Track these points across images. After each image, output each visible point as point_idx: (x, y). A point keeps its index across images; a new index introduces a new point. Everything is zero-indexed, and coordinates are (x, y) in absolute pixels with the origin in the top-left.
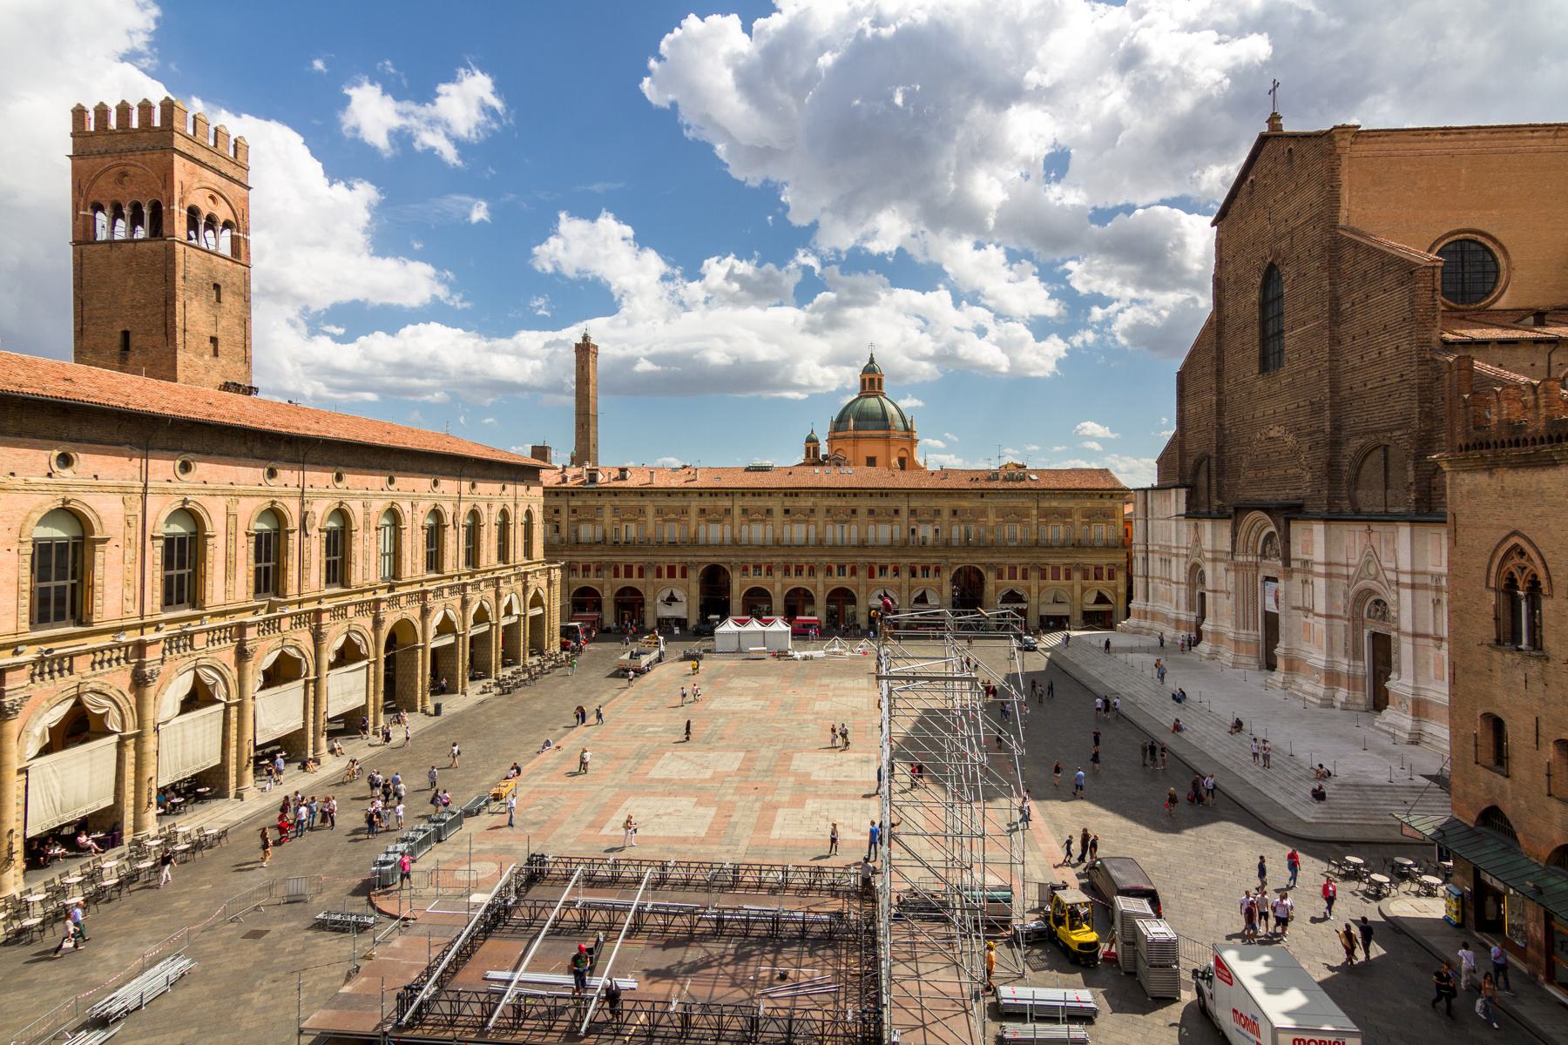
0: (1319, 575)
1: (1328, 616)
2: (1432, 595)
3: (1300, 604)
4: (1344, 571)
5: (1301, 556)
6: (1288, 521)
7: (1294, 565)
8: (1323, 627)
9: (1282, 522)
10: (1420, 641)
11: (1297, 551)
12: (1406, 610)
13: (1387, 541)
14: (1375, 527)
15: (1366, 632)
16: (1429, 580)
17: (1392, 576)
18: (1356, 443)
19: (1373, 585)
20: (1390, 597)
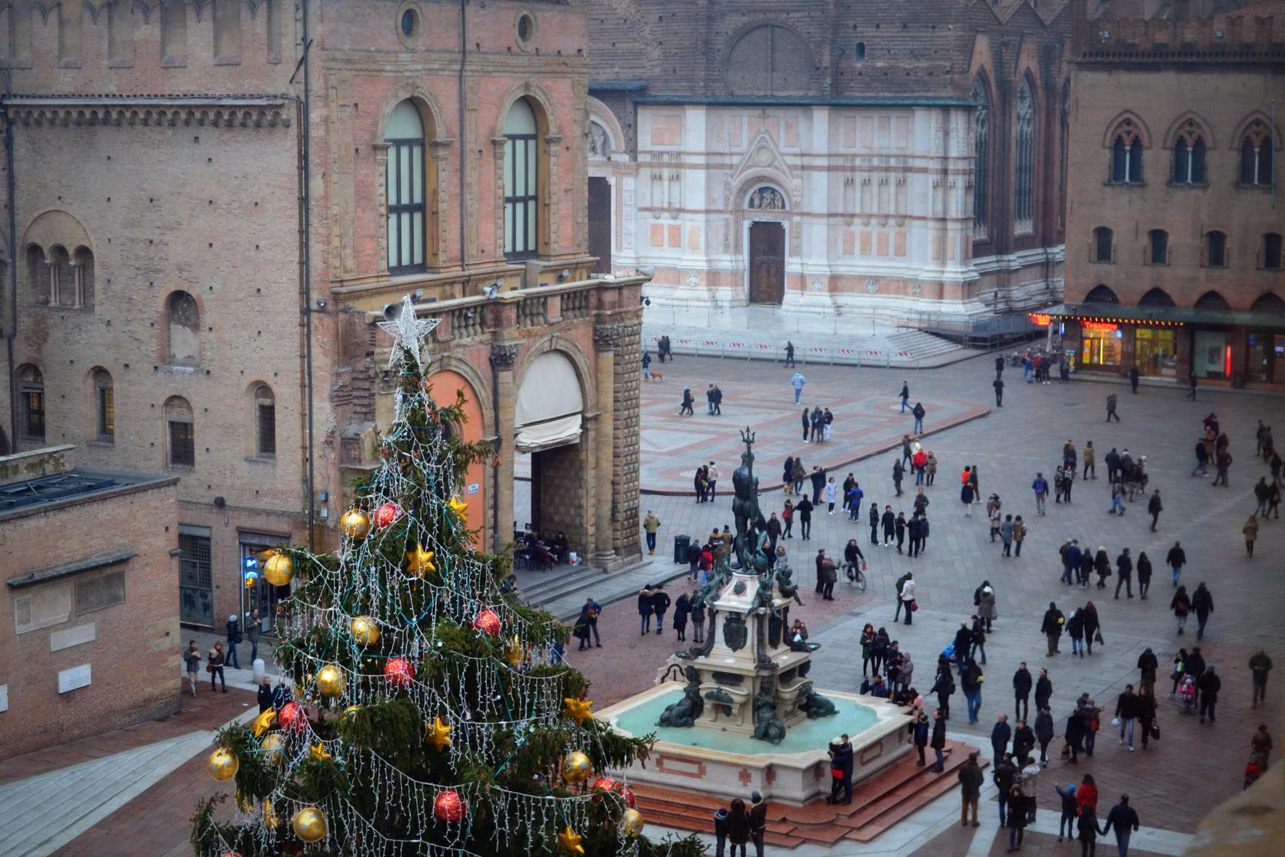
0: (695, 167)
1: (707, 212)
2: (841, 176)
3: (648, 205)
4: (727, 160)
5: (649, 147)
6: (636, 104)
7: (641, 158)
8: (702, 226)
9: (630, 108)
10: (833, 220)
11: (645, 142)
12: (817, 192)
13: (788, 126)
14: (771, 112)
15: (746, 224)
16: (840, 162)
17: (798, 161)
18: (732, 23)
19: (768, 172)
20: (792, 183)
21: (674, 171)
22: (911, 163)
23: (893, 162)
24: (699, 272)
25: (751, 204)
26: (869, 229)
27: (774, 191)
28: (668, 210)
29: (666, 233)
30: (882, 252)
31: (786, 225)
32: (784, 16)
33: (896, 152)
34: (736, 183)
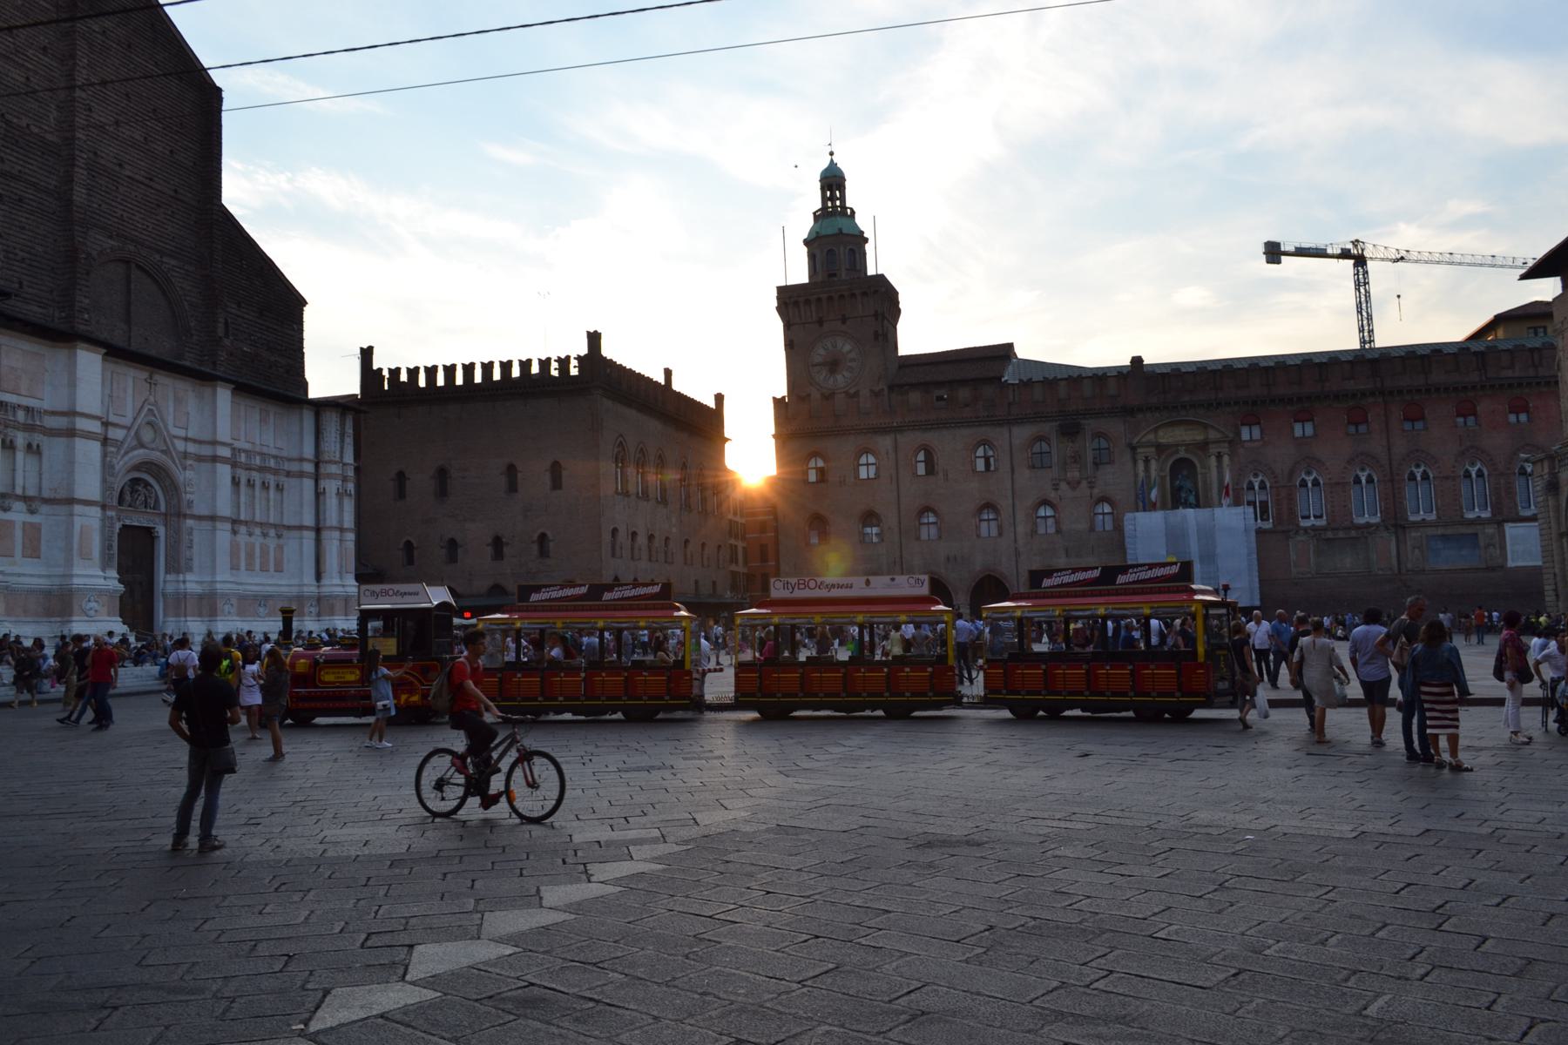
0: (88, 435)
12: (212, 491)
13: (178, 401)
14: (162, 379)
15: (118, 526)
21: (37, 438)
22: (286, 466)
23: (272, 463)
24: (101, 593)
25: (121, 500)
26: (252, 539)
27: (147, 484)
28: (25, 499)
29: (19, 533)
30: (264, 569)
31: (161, 531)
32: (157, 257)
33: (274, 452)
34: (122, 463)
